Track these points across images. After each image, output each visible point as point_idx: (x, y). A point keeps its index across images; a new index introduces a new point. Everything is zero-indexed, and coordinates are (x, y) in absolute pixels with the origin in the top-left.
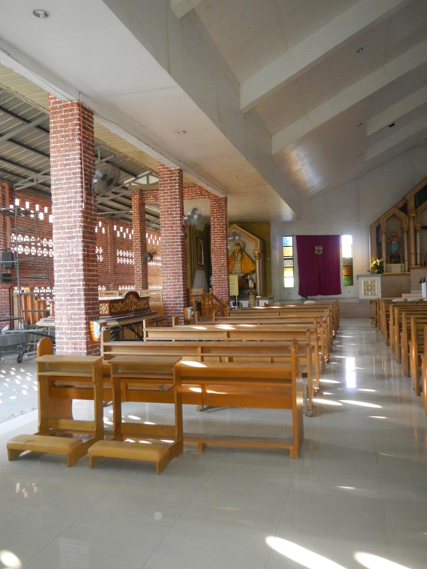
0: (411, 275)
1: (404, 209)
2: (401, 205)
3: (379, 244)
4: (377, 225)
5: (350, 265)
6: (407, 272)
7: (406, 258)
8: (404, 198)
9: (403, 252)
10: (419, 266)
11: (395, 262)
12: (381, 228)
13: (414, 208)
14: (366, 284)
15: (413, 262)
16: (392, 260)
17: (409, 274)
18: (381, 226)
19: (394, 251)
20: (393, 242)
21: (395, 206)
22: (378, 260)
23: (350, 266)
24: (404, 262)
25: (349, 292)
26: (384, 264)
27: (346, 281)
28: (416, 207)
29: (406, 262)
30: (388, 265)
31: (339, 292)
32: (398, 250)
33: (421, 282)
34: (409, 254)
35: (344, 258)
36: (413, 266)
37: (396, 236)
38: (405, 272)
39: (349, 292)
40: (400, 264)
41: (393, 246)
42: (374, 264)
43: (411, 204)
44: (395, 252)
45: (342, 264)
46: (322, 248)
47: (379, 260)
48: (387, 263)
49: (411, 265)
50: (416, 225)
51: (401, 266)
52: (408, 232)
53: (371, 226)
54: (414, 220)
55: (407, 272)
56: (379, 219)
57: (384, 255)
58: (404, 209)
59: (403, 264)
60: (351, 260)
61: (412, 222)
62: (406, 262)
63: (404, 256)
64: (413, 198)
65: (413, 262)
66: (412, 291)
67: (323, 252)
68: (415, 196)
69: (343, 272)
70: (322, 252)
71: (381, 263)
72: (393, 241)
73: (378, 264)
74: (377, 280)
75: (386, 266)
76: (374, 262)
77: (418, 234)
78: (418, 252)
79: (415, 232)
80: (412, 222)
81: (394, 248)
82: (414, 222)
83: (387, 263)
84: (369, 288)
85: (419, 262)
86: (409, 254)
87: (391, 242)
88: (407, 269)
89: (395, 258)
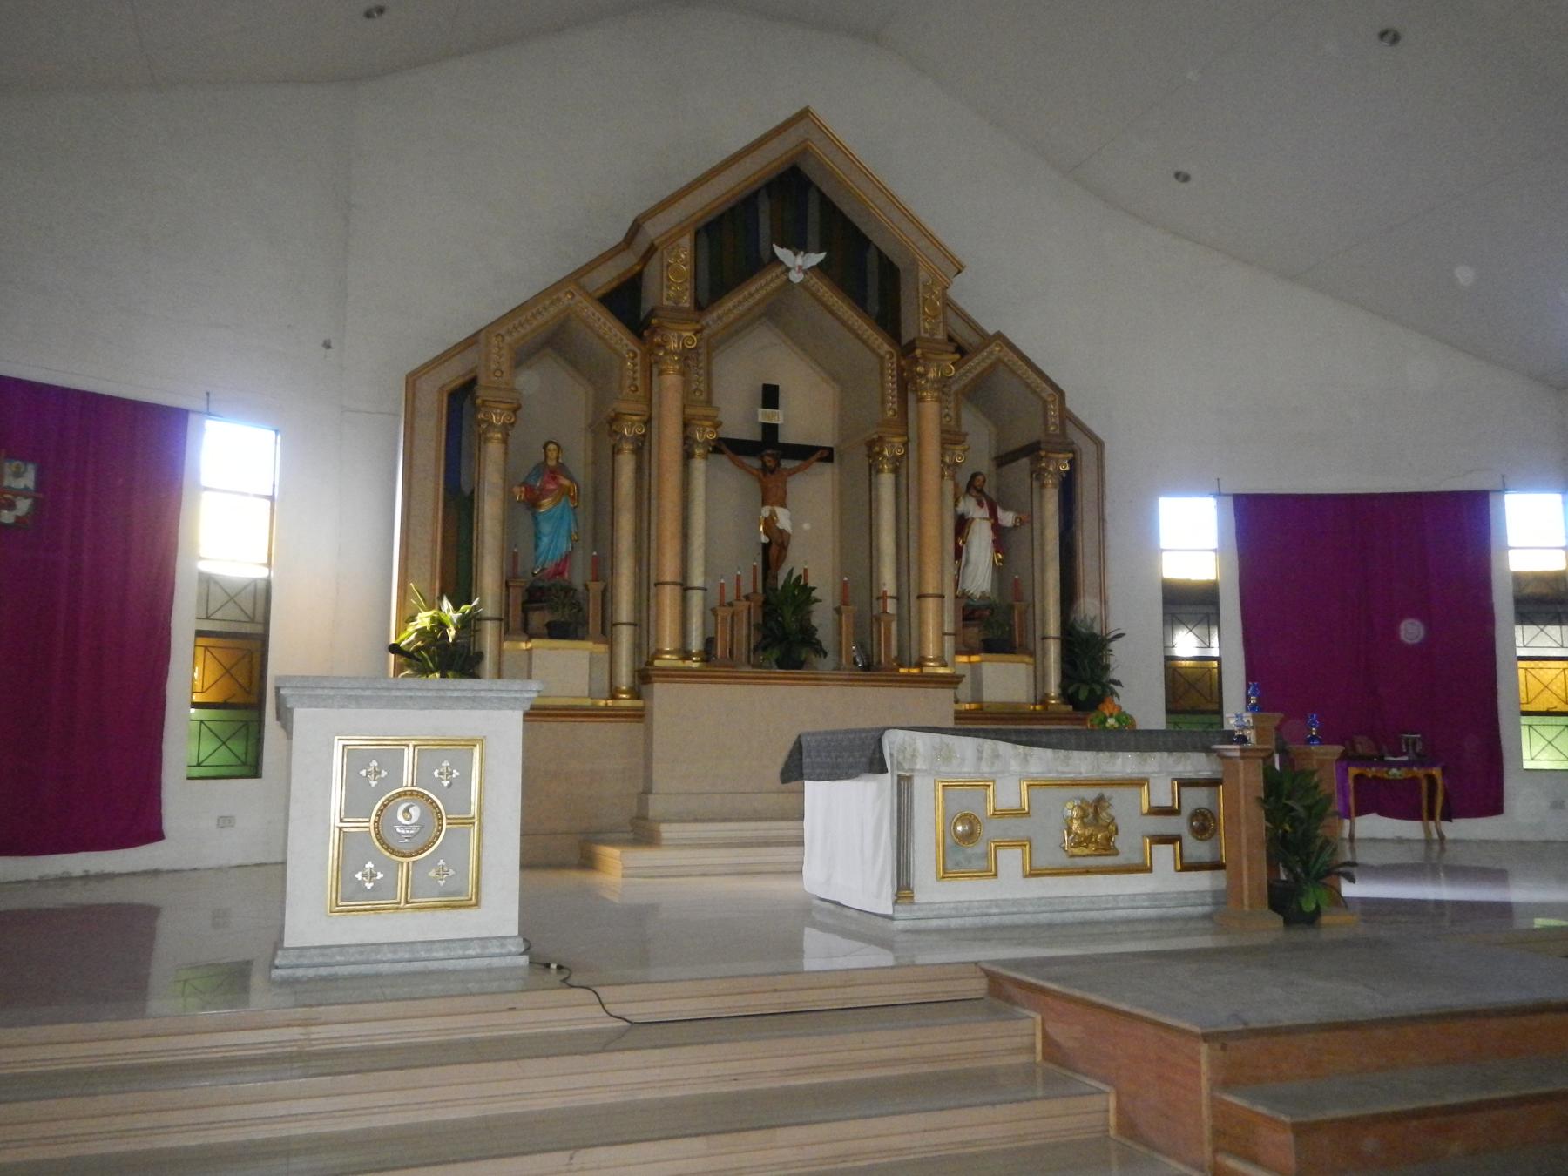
1: (626, 301)
2: (605, 278)
3: (459, 507)
4: (451, 375)
5: (247, 628)
6: (625, 701)
7: (624, 610)
8: (636, 228)
9: (603, 568)
10: (694, 664)
11: (558, 631)
12: (482, 393)
13: (686, 302)
14: (369, 777)
15: (669, 641)
16: (538, 619)
17: (639, 715)
18: (482, 381)
19: (549, 565)
20: (546, 504)
21: (575, 278)
22: (446, 604)
23: (244, 644)
24: (606, 633)
25: (225, 822)
26: (490, 633)
27: (208, 746)
28: (700, 307)
29: (625, 636)
30: (506, 645)
31: (139, 821)
32: (567, 558)
33: (795, 769)
34: (646, 586)
35: (207, 581)
36: (669, 661)
37: (561, 469)
38: (614, 695)
39: (225, 822)
40: (589, 645)
41: (546, 528)
42: (421, 633)
44: (558, 572)
45: (184, 622)
46: (28, 480)
47: (456, 608)
48: (507, 632)
49: (659, 653)
50: (688, 411)
52: (642, 448)
53: (412, 380)
54: (683, 373)
55: (625, 701)
56: (471, 341)
58: (626, 301)
59: (602, 648)
60: (262, 596)
61: (671, 381)
62: (625, 636)
63: (607, 598)
64: (686, 241)
65: (669, 641)
66: (667, 831)
67: (38, 505)
68: (697, 233)
69: (191, 677)
70: (23, 506)
71: (469, 625)
72: (543, 493)
73: (451, 633)
74: (484, 742)
75: (500, 653)
76: (424, 620)
77: (699, 465)
78: (697, 579)
79: (688, 456)
80: (671, 381)
81: (555, 539)
82: (686, 383)
83: (507, 632)
84: (407, 818)
85: (696, 644)
86: (646, 586)
87: (532, 503)
88: (624, 679)
89: (552, 607)
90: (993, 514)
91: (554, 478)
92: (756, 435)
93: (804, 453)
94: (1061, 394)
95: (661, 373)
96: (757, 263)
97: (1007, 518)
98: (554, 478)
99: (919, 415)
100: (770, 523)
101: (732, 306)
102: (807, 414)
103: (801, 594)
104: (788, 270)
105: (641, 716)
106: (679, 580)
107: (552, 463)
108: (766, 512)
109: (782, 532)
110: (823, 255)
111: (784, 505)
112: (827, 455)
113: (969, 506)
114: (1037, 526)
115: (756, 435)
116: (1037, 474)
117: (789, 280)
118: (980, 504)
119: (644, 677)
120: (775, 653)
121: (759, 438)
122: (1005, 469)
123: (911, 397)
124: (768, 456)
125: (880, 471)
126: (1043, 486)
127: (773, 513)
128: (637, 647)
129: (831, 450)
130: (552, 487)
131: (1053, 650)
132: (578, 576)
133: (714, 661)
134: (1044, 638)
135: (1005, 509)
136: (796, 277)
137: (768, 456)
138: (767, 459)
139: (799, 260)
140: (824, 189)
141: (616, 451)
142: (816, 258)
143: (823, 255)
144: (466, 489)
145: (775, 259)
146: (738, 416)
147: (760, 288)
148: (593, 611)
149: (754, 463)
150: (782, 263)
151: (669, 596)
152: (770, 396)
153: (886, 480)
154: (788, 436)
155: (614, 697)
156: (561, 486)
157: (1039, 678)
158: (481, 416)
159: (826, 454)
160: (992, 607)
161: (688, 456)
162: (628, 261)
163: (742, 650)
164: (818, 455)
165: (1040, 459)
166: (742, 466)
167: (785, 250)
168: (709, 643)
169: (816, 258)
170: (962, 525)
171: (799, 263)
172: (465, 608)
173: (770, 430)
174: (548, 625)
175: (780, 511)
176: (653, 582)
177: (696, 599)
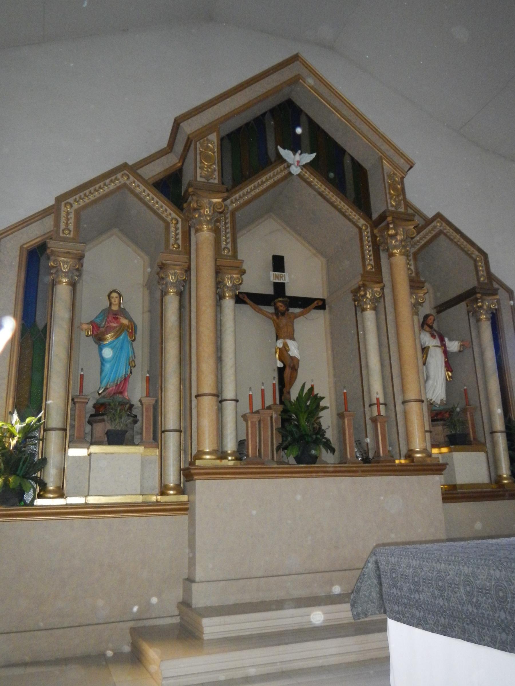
0: (199, 510)
2: (156, 170)
4: (32, 235)
6: (172, 497)
7: (171, 420)
10: (230, 462)
11: (115, 438)
16: (100, 429)
22: (15, 417)
24: (156, 439)
29: (172, 440)
37: (123, 312)
40: (139, 450)
43: (204, 168)
47: (22, 419)
49: (200, 454)
51: (143, 456)
57: (55, 398)
61: (205, 236)
63: (157, 410)
64: (213, 137)
66: (211, 627)
78: (229, 392)
79: (220, 297)
85: (230, 446)
86: (188, 397)
88: (172, 479)
90: (443, 345)
91: (116, 319)
92: (270, 291)
93: (305, 303)
94: (485, 255)
95: (197, 231)
96: (267, 162)
97: (453, 346)
98: (116, 319)
99: (391, 266)
100: (283, 352)
101: (250, 190)
102: (304, 278)
103: (312, 402)
104: (289, 166)
105: (186, 509)
106: (214, 392)
107: (115, 308)
108: (280, 344)
109: (293, 358)
110: (314, 155)
111: (293, 338)
112: (321, 305)
113: (427, 339)
114: (476, 349)
115: (270, 291)
116: (474, 313)
117: (290, 173)
118: (433, 336)
119: (188, 474)
120: (295, 451)
121: (272, 293)
122: (443, 314)
123: (383, 256)
124: (279, 304)
125: (363, 310)
126: (478, 320)
127: (285, 345)
128: (182, 449)
129: (323, 300)
130: (114, 325)
131: (501, 441)
132: (137, 392)
133: (246, 461)
134: (492, 433)
135: (450, 340)
136: (295, 170)
137: (279, 304)
138: (279, 304)
139: (297, 157)
140: (310, 114)
141: (164, 293)
142: (308, 158)
143: (314, 155)
144: (40, 325)
145: (281, 160)
146: (258, 279)
147: (268, 178)
148: (145, 422)
149: (270, 310)
150: (284, 161)
151: (208, 404)
152: (278, 264)
153: (369, 315)
154: (290, 292)
155: (163, 493)
156: (122, 325)
157: (493, 464)
158: (52, 264)
159: (320, 303)
160: (451, 411)
161: (220, 297)
162: (171, 161)
163: (267, 450)
164: (315, 304)
165: (476, 300)
166: (260, 312)
167: (286, 151)
168: (241, 444)
169: (308, 158)
170: (425, 350)
171: (297, 160)
172: (31, 420)
173: (280, 288)
174: (108, 433)
175: (290, 342)
176: (194, 393)
177: (229, 408)
